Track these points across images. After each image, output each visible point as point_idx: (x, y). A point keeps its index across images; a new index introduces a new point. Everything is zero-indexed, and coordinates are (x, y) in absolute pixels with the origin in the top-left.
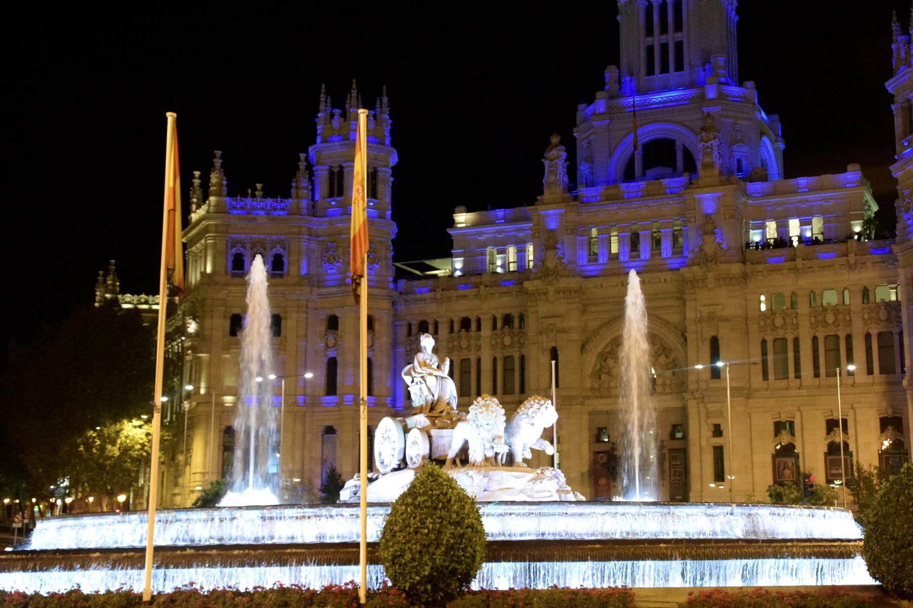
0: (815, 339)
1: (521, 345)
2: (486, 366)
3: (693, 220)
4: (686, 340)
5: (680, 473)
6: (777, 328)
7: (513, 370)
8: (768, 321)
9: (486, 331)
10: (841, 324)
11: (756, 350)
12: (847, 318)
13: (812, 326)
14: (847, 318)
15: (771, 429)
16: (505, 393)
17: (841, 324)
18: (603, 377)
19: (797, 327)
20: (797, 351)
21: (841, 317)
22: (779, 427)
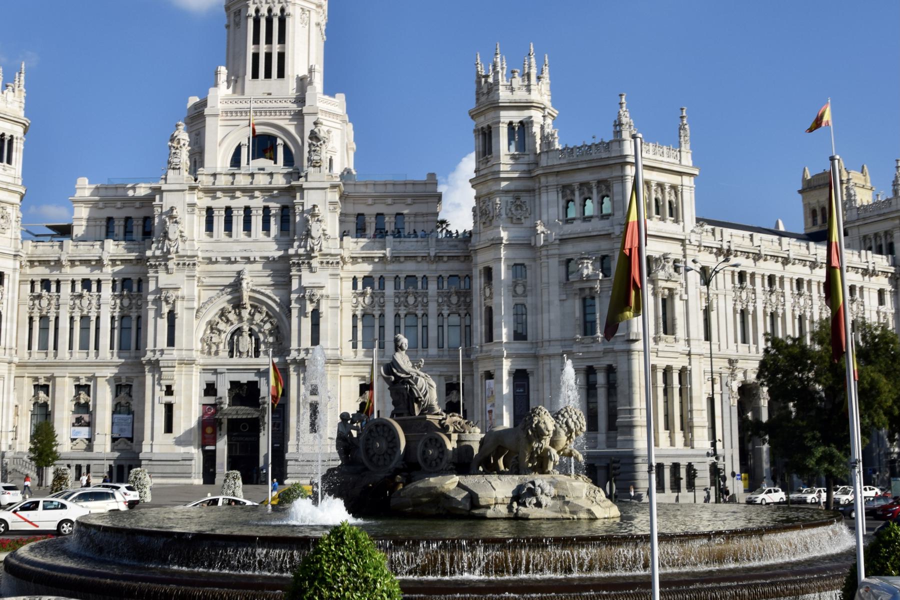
0: (397, 315)
1: (139, 307)
2: (64, 324)
5: (279, 424)
7: (130, 328)
10: (420, 305)
12: (425, 300)
13: (397, 305)
14: (425, 300)
16: (121, 348)
17: (420, 305)
18: (214, 340)
20: (382, 327)
21: (420, 299)
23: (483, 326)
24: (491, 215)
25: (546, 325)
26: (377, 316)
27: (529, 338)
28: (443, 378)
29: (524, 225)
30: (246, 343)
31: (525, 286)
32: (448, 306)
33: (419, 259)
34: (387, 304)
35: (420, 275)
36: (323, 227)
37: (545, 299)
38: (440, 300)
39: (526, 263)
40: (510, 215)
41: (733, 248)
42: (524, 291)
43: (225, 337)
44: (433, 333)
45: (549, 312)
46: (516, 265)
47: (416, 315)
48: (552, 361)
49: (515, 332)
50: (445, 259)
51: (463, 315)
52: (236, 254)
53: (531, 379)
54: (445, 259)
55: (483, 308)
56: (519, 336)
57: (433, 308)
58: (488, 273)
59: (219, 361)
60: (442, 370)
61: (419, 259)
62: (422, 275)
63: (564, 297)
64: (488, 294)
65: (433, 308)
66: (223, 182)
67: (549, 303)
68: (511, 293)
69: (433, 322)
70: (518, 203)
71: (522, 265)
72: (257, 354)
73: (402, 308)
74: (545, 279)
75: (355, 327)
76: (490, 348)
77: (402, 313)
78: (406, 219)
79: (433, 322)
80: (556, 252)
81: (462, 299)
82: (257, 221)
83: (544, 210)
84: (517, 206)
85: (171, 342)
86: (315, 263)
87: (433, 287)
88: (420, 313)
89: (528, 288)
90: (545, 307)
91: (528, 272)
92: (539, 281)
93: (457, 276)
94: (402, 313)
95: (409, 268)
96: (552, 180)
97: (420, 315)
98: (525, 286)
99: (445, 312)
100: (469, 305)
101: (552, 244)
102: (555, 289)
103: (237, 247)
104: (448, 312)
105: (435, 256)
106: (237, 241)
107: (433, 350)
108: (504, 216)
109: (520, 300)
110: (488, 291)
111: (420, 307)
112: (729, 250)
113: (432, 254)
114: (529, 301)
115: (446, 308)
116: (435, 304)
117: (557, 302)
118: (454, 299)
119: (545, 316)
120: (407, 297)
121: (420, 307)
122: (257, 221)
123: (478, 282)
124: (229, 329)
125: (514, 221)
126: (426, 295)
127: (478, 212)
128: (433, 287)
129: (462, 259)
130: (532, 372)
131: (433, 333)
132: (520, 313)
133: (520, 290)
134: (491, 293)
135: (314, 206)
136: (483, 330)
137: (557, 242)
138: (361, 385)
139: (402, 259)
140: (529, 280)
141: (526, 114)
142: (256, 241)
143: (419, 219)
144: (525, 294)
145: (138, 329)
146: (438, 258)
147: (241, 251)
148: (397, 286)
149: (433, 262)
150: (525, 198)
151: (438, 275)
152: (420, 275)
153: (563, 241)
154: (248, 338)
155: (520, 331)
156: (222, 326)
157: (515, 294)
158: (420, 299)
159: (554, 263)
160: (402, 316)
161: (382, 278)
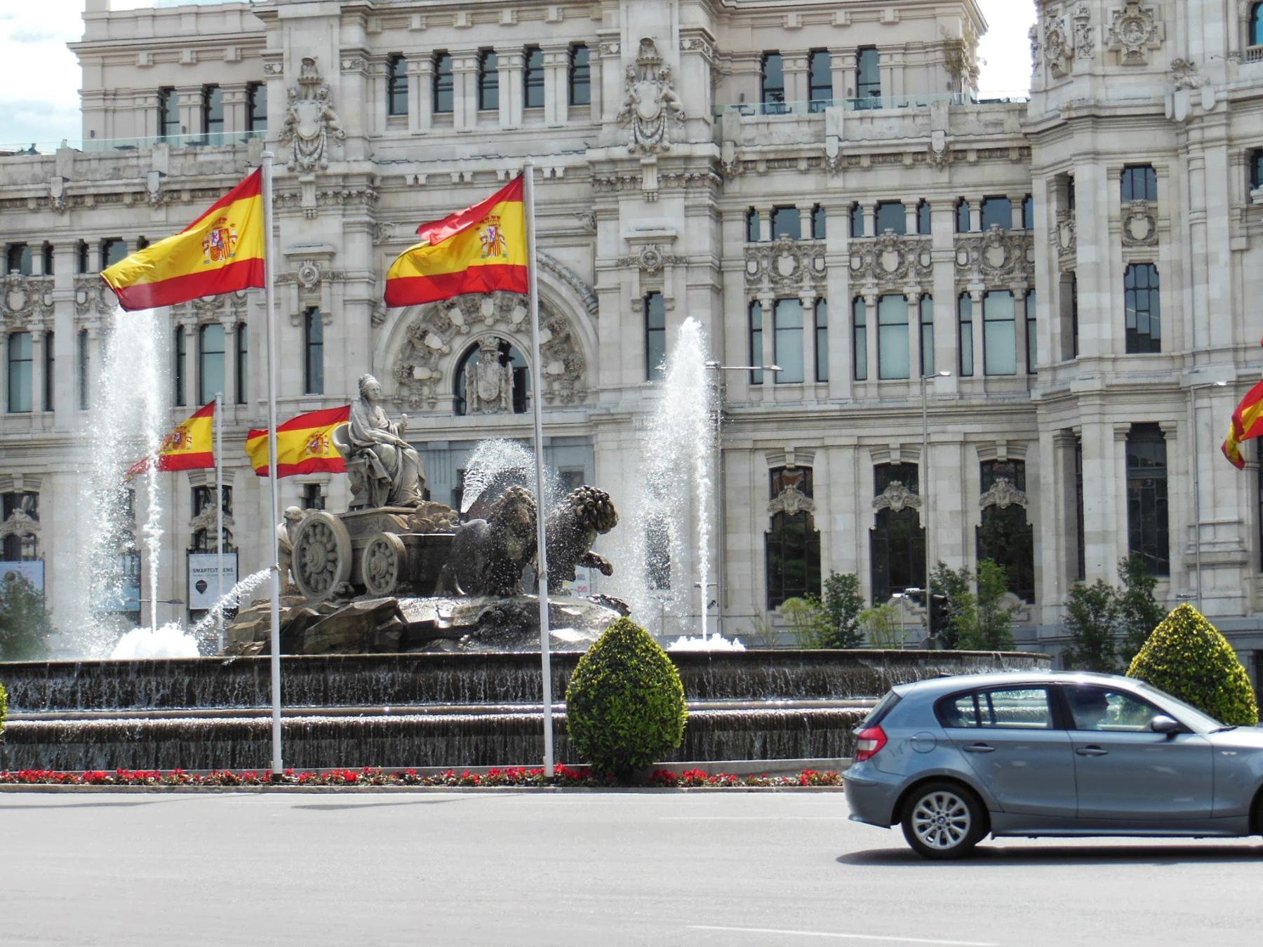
0: (857, 300)
3: (614, 48)
4: (595, 299)
6: (783, 278)
8: (765, 263)
10: (912, 274)
11: (738, 321)
12: (925, 260)
13: (854, 274)
14: (925, 260)
15: (764, 481)
17: (912, 274)
18: (419, 373)
19: (820, 277)
20: (819, 329)
21: (911, 258)
22: (779, 479)
23: (1058, 321)
24: (1069, 43)
25: (1201, 311)
26: (808, 303)
27: (1165, 346)
28: (972, 452)
29: (1149, 69)
30: (490, 378)
31: (1151, 220)
32: (981, 271)
33: (908, 160)
34: (831, 272)
35: (911, 198)
36: (666, 90)
37: (1198, 248)
38: (962, 259)
39: (1155, 163)
40: (1111, 44)
42: (1151, 231)
43: (448, 365)
44: (944, 338)
45: (1207, 282)
46: (1129, 167)
47: (906, 299)
48: (1216, 402)
49: (1131, 334)
50: (972, 157)
51: (1019, 294)
52: (462, 166)
53: (1171, 447)
54: (972, 157)
55: (1057, 277)
56: (1141, 341)
57: (944, 281)
58: (1066, 185)
59: (431, 422)
60: (969, 428)
61: (908, 160)
62: (916, 199)
63: (1241, 243)
64: (1065, 242)
65: (944, 281)
67: (1207, 259)
68: (1118, 238)
69: (943, 313)
70: (1133, 12)
71: (1147, 166)
72: (520, 403)
73: (870, 281)
74: (1198, 203)
75: (753, 331)
76: (1074, 372)
77: (870, 291)
78: (884, 59)
79: (943, 313)
80: (1220, 132)
81: (1017, 253)
82: (510, 85)
83: (1194, 31)
84: (1130, 20)
85: (312, 381)
86: (650, 181)
87: (943, 225)
88: (912, 292)
89: (1160, 224)
90: (1199, 268)
91: (1162, 185)
92: (1185, 205)
93: (1004, 197)
94: (870, 293)
95: (886, 182)
97: (913, 298)
98: (1151, 220)
99: (976, 289)
100: (1028, 267)
101: (1212, 112)
102: (1219, 223)
103: (464, 149)
104: (982, 287)
105: (947, 151)
106: (467, 134)
107: (945, 382)
108: (1099, 48)
110: (1065, 234)
111: (912, 277)
113: (939, 146)
114: (1165, 255)
115: (975, 276)
116: (950, 269)
117: (1224, 256)
118: (996, 256)
119: (1200, 289)
120: (879, 255)
121: (912, 277)
122: (510, 85)
123: (1044, 212)
124: (460, 346)
125: (1124, 59)
126: (925, 248)
127: (1042, 39)
128: (943, 225)
129: (1014, 155)
130: (1173, 430)
131: (944, 338)
132: (1141, 283)
133: (1139, 228)
134: (1073, 239)
135: (647, 43)
136: (1058, 330)
137: (1223, 107)
138: (773, 471)
139: (866, 162)
140: (1165, 202)
142: (510, 131)
143: (913, 58)
144: (1152, 239)
145: (240, 353)
146: (953, 157)
147: (475, 158)
148: (854, 229)
149: (941, 166)
151: (953, 197)
153: (1238, 104)
154: (496, 365)
155: (1143, 329)
156: (434, 341)
157: (1129, 240)
158: (911, 258)
159: (1217, 158)
160: (870, 300)
161: (816, 209)
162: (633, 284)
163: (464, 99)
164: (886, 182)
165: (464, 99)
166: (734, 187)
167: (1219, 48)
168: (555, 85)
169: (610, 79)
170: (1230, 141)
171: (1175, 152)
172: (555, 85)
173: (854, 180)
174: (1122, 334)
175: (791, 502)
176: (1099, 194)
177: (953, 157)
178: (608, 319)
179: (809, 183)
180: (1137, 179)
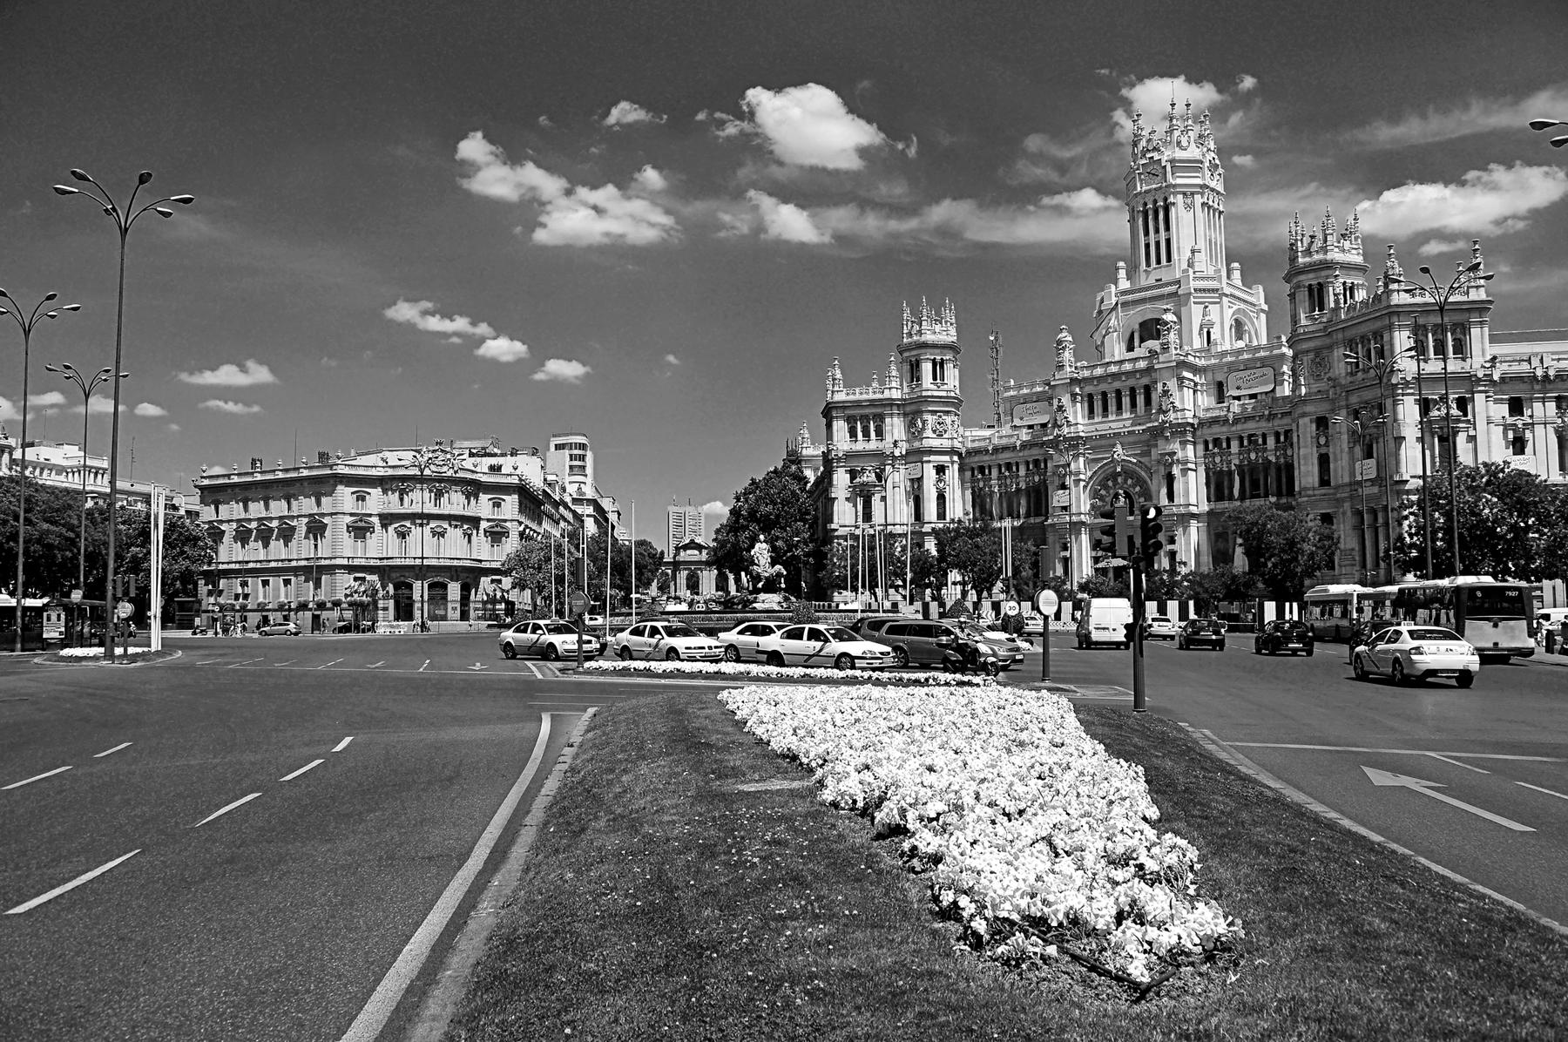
9: (1022, 472)
35: (1259, 432)
41: (1552, 373)
66: (1113, 369)
87: (1271, 442)
95: (1251, 426)
96: (1340, 336)
109: (1323, 450)
112: (1546, 377)
122: (1126, 401)
126: (1265, 450)
128: (1271, 442)
132: (1324, 461)
133: (1322, 441)
141: (1324, 273)
144: (1327, 445)
150: (1325, 352)
152: (1259, 432)
157: (1319, 446)
162: (1162, 471)
163: (1112, 407)
164: (1251, 426)
165: (1112, 407)
166: (1198, 433)
167: (1343, 372)
168: (1140, 400)
169: (1154, 396)
170: (1347, 407)
171: (1333, 411)
172: (1140, 400)
173: (1239, 427)
174: (1317, 479)
175: (1221, 545)
176: (1307, 428)
177: (1271, 417)
178: (1155, 481)
179: (1224, 429)
180: (1322, 423)
